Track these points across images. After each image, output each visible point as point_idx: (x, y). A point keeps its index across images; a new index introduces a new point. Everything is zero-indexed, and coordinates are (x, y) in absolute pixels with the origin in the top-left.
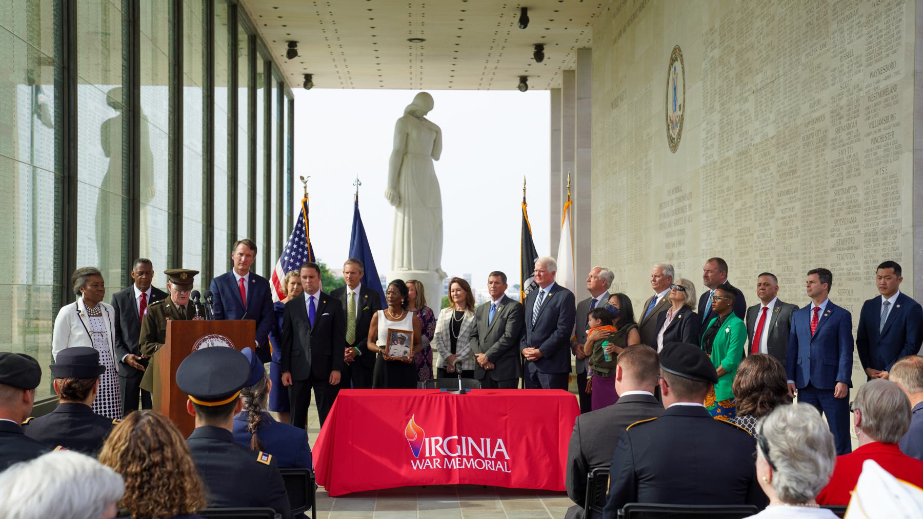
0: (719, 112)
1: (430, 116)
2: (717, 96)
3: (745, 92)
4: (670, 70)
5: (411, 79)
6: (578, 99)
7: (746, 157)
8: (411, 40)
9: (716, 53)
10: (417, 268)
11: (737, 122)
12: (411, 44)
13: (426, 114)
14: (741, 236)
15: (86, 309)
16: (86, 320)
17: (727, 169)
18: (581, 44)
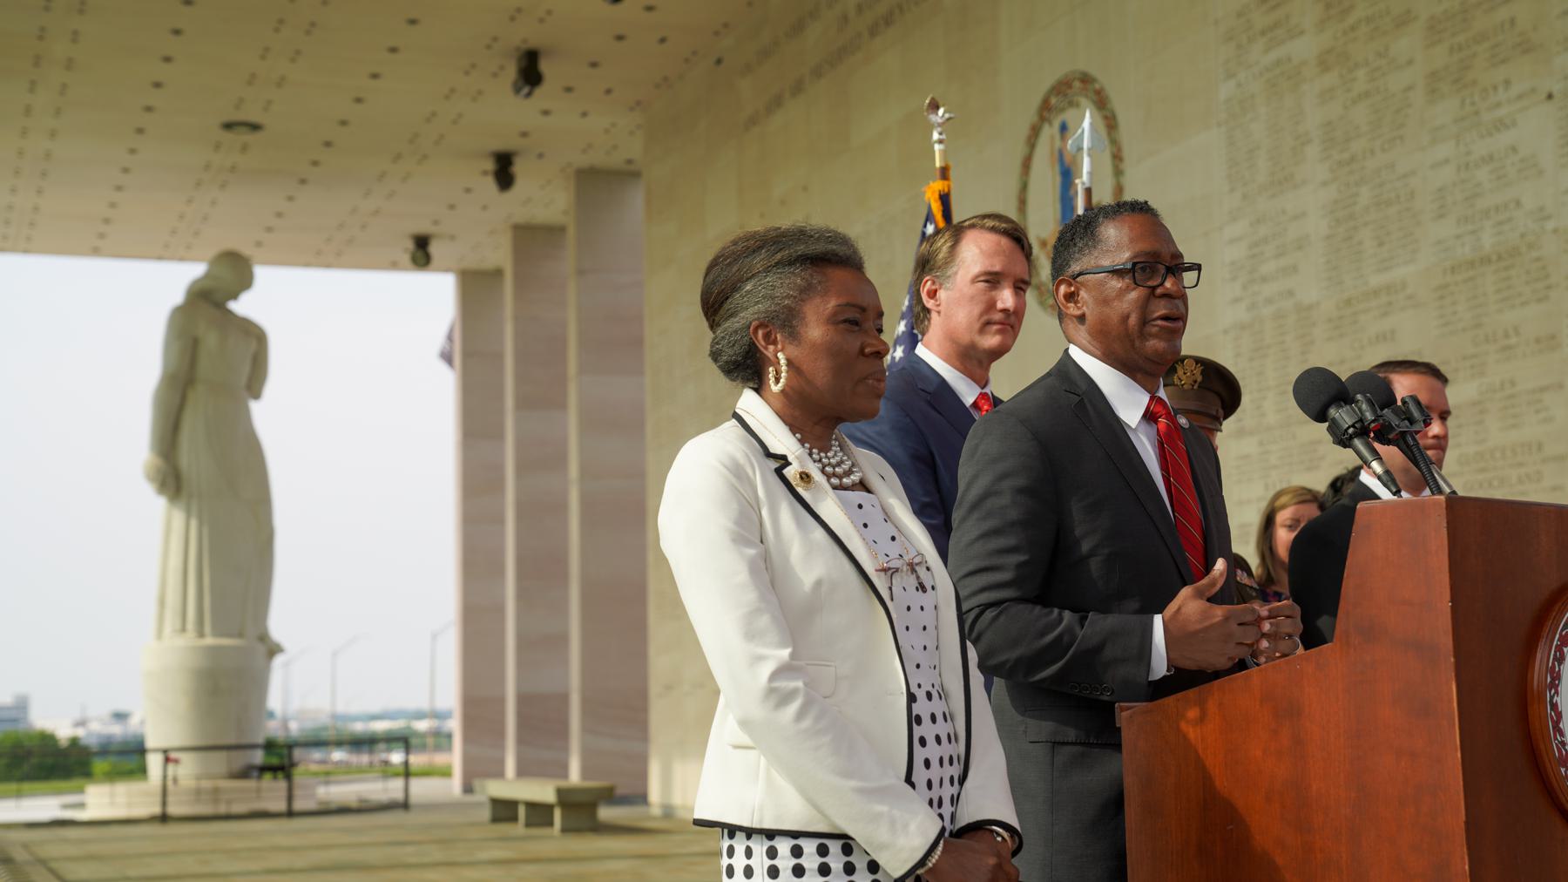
0: (1325, 184)
1: (242, 306)
2: (1313, 151)
3: (1498, 105)
4: (1035, 132)
5: (174, 232)
6: (581, 272)
7: (1507, 268)
8: (229, 126)
9: (1304, 48)
10: (217, 633)
11: (1440, 190)
12: (228, 137)
13: (235, 296)
14: (1483, 470)
15: (810, 454)
16: (830, 507)
17: (1385, 314)
18: (584, 161)
